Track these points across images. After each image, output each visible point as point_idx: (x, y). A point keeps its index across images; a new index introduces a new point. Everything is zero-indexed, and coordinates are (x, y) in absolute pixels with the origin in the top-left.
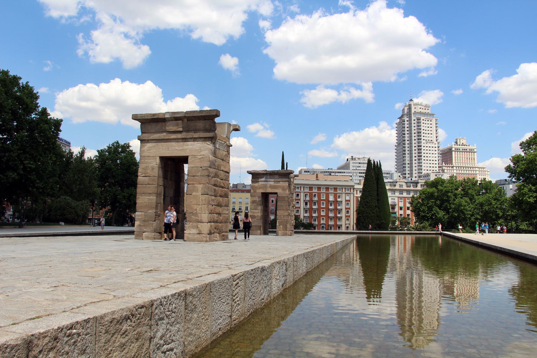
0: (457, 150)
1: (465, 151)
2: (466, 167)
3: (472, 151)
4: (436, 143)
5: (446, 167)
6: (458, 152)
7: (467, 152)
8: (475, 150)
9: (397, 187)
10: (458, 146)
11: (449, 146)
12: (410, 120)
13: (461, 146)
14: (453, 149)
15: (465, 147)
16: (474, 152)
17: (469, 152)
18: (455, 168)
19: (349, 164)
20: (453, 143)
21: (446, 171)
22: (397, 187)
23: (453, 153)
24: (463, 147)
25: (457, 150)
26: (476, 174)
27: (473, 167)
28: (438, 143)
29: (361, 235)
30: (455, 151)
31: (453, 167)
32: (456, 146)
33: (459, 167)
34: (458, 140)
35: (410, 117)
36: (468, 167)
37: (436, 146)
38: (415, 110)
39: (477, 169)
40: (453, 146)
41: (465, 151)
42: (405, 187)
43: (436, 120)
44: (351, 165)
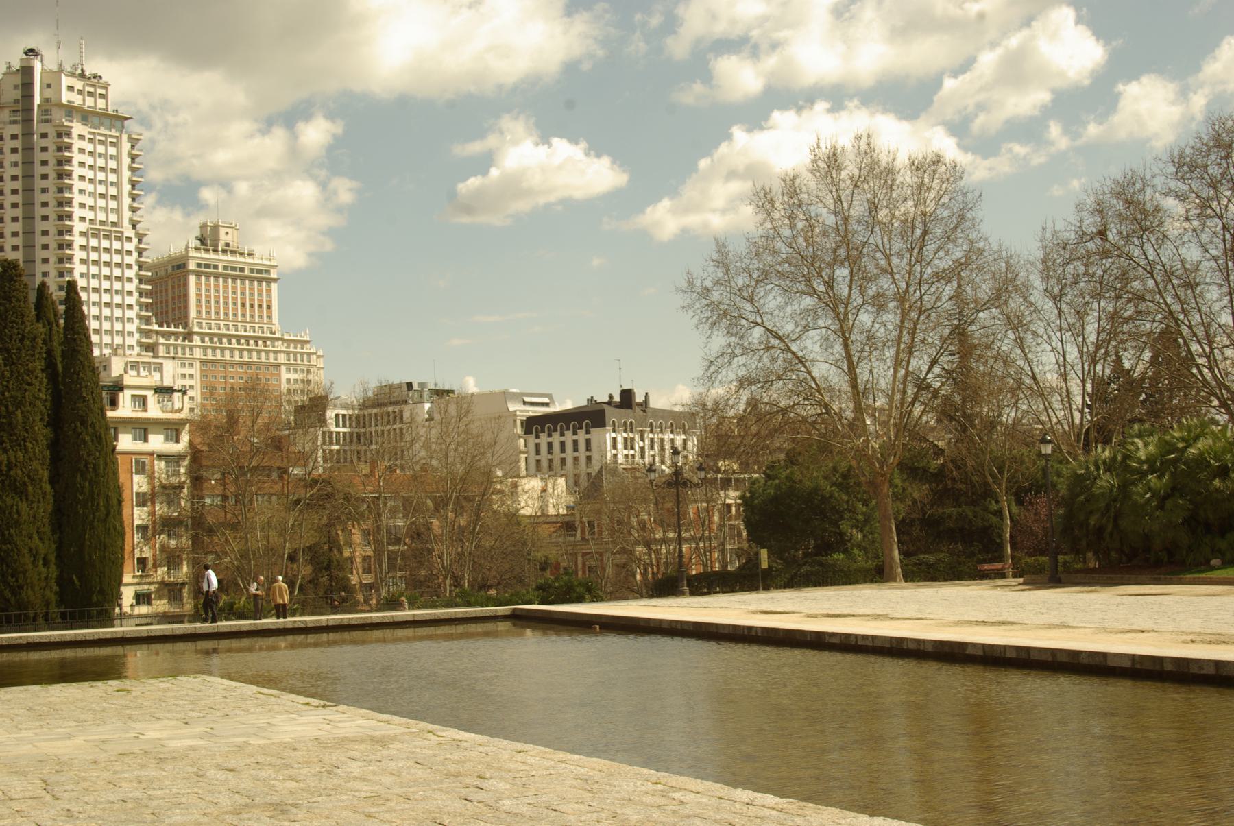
0: (207, 270)
2: (238, 338)
5: (164, 334)
6: (208, 276)
8: (273, 275)
10: (212, 256)
14: (192, 266)
15: (240, 259)
16: (269, 281)
17: (252, 280)
18: (197, 340)
20: (194, 243)
21: (162, 351)
23: (192, 279)
24: (230, 257)
25: (207, 270)
26: (278, 366)
27: (265, 339)
29: (69, 653)
30: (199, 275)
31: (188, 336)
32: (203, 255)
33: (212, 336)
36: (247, 338)
38: (49, 93)
39: (280, 346)
40: (192, 253)
41: (235, 273)
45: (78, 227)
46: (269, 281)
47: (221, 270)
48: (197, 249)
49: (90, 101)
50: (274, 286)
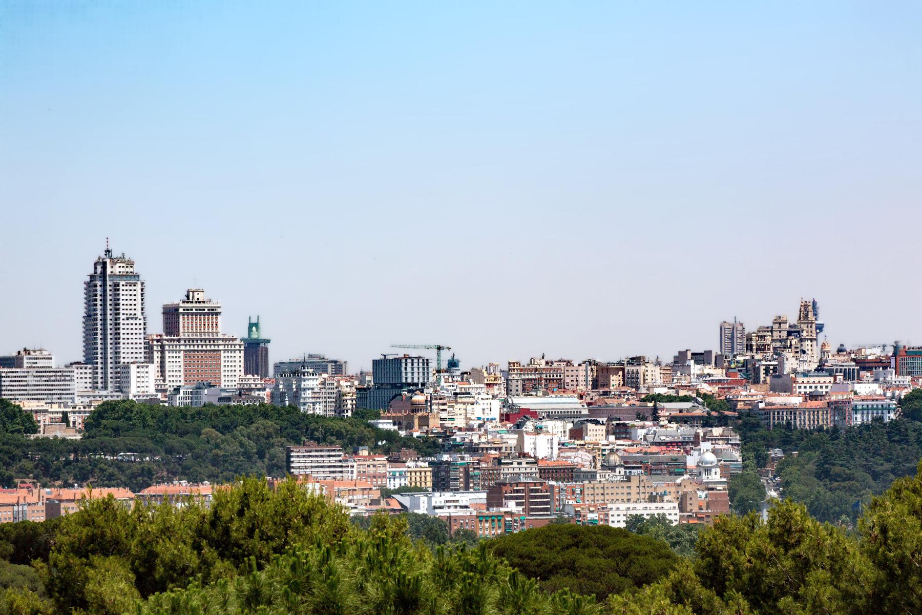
1: (200, 313)
3: (214, 313)
4: (140, 316)
5: (167, 340)
6: (188, 314)
7: (204, 314)
8: (219, 310)
9: (77, 409)
11: (176, 302)
12: (104, 285)
13: (194, 305)
14: (181, 310)
15: (202, 305)
16: (217, 314)
18: (182, 342)
19: (22, 359)
22: (77, 409)
23: (181, 317)
24: (198, 305)
25: (188, 313)
28: (144, 318)
30: (184, 314)
31: (179, 340)
32: (186, 305)
34: (191, 294)
35: (104, 281)
37: (142, 322)
39: (220, 342)
42: (82, 409)
43: (142, 284)
44: (25, 361)
45: (122, 317)
46: (217, 314)
47: (194, 311)
48: (184, 302)
49: (127, 270)
50: (219, 317)
